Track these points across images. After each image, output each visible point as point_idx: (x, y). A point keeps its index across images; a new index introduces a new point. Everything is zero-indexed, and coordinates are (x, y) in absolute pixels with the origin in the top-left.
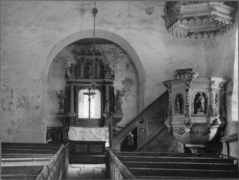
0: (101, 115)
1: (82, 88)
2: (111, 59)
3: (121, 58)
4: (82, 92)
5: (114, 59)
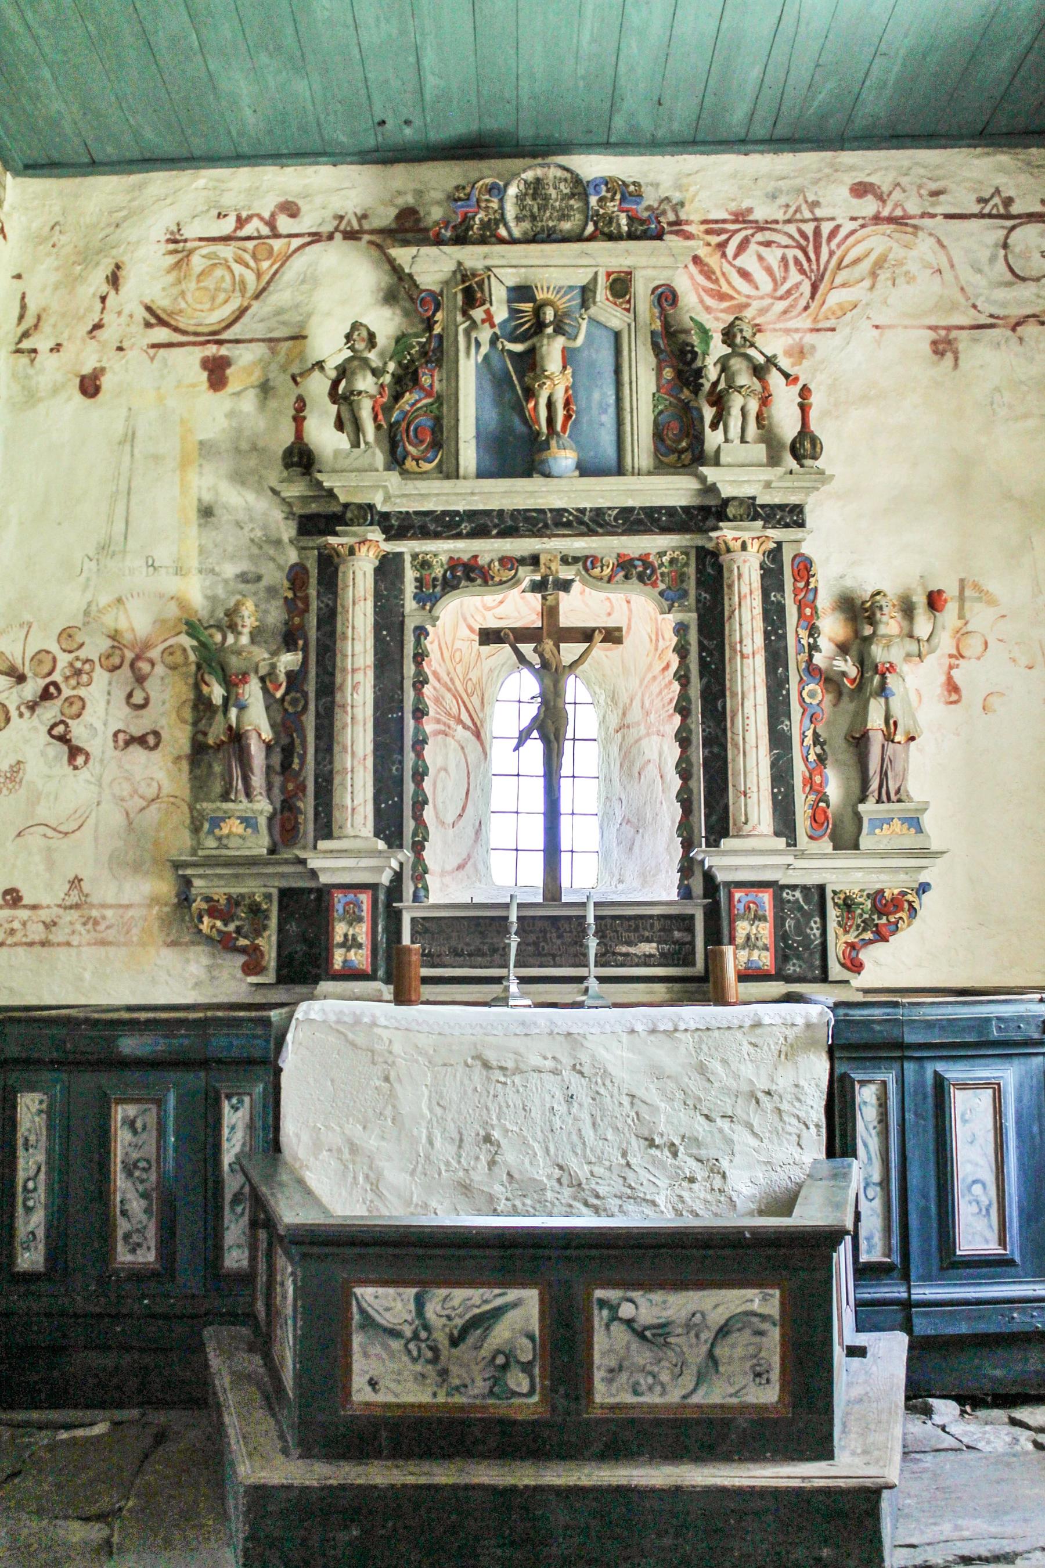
0: (687, 867)
1: (468, 574)
3: (874, 275)
5: (797, 286)
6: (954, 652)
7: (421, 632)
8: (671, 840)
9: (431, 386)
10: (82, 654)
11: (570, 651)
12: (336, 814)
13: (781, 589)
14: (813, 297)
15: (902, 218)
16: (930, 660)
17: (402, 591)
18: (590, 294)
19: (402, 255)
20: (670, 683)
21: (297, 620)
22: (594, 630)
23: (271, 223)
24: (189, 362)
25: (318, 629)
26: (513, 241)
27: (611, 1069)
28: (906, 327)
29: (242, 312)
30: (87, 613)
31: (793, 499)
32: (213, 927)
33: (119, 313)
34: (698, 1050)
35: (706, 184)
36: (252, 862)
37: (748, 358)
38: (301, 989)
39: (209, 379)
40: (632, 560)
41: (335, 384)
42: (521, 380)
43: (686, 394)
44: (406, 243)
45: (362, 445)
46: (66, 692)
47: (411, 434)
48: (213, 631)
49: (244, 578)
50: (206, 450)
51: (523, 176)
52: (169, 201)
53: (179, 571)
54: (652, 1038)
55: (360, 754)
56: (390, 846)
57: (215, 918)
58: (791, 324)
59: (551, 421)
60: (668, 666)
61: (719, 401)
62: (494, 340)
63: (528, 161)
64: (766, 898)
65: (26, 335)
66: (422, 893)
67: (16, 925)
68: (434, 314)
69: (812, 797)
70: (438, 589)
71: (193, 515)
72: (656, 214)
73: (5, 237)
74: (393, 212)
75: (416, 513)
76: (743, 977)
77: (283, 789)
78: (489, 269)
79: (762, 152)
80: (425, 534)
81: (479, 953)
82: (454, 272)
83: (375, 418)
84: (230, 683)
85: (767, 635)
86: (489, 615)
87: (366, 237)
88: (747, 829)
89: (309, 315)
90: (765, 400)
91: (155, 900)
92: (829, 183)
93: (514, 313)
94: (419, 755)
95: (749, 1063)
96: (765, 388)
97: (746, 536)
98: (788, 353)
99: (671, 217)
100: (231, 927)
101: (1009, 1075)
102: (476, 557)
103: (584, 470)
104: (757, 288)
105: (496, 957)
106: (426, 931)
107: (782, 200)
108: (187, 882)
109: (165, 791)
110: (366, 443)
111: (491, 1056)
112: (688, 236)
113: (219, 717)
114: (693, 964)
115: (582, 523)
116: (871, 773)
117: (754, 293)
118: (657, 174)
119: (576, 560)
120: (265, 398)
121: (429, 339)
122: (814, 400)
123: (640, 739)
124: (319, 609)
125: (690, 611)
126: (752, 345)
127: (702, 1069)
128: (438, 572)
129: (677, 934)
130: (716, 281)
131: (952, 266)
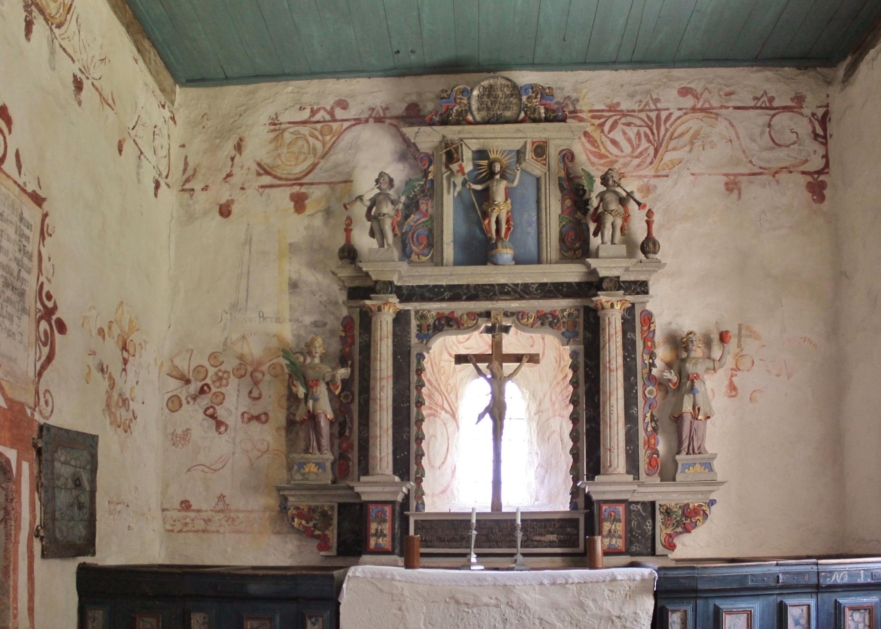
0: (575, 492)
2: (627, 148)
3: (692, 143)
4: (443, 348)
5: (646, 149)
6: (734, 367)
7: (420, 357)
8: (566, 476)
9: (427, 210)
10: (223, 368)
11: (509, 367)
12: (371, 461)
13: (634, 331)
14: (655, 156)
15: (709, 109)
16: (721, 372)
17: (409, 333)
18: (522, 155)
19: (410, 132)
20: (567, 386)
21: (347, 349)
22: (522, 355)
23: (331, 113)
24: (282, 197)
25: (360, 354)
26: (476, 123)
27: (529, 604)
28: (710, 174)
29: (314, 166)
30: (225, 344)
31: (642, 278)
32: (300, 524)
33: (242, 167)
34: (579, 594)
35: (592, 88)
36: (323, 487)
37: (616, 193)
38: (353, 559)
39: (295, 207)
40: (545, 314)
41: (370, 209)
42: (480, 206)
43: (579, 215)
44: (412, 125)
45: (386, 246)
46: (214, 390)
47: (415, 239)
48: (299, 355)
49: (315, 324)
50: (293, 248)
51: (482, 84)
52: (270, 101)
53: (278, 320)
54: (553, 587)
55: (385, 426)
56: (402, 479)
57: (302, 519)
58: (643, 173)
59: (498, 231)
60: (566, 376)
61: (599, 219)
62: (464, 183)
63: (485, 74)
64: (621, 509)
65: (187, 181)
66: (421, 507)
67: (188, 520)
68: (428, 167)
69: (649, 452)
70: (430, 332)
71: (286, 287)
72: (562, 106)
73: (175, 123)
74: (404, 106)
75: (418, 286)
76: (606, 553)
77: (340, 447)
78: (461, 140)
79: (626, 69)
80: (423, 299)
81: (453, 540)
82: (441, 142)
83: (393, 230)
84: (307, 385)
85: (625, 358)
86: (461, 346)
87: (388, 121)
88: (611, 470)
89: (354, 168)
90: (626, 218)
91: (266, 509)
92: (667, 88)
93: (477, 166)
94: (419, 428)
95: (609, 602)
96: (626, 211)
97: (614, 299)
98: (640, 190)
99: (571, 108)
100: (311, 524)
101: (756, 606)
102: (453, 312)
103: (518, 261)
104: (622, 151)
105: (464, 542)
106: (423, 527)
107: (638, 98)
108: (285, 499)
109: (271, 447)
110: (388, 245)
111: (460, 597)
112: (581, 120)
113: (302, 405)
114: (578, 546)
115: (516, 292)
116: (684, 437)
117: (620, 154)
118: (563, 82)
119: (512, 314)
120: (328, 218)
121: (425, 182)
122: (656, 218)
123: (549, 419)
124: (360, 343)
125: (580, 344)
126: (619, 185)
127: (581, 605)
128: (431, 321)
129: (568, 530)
130: (598, 147)
131: (738, 138)
